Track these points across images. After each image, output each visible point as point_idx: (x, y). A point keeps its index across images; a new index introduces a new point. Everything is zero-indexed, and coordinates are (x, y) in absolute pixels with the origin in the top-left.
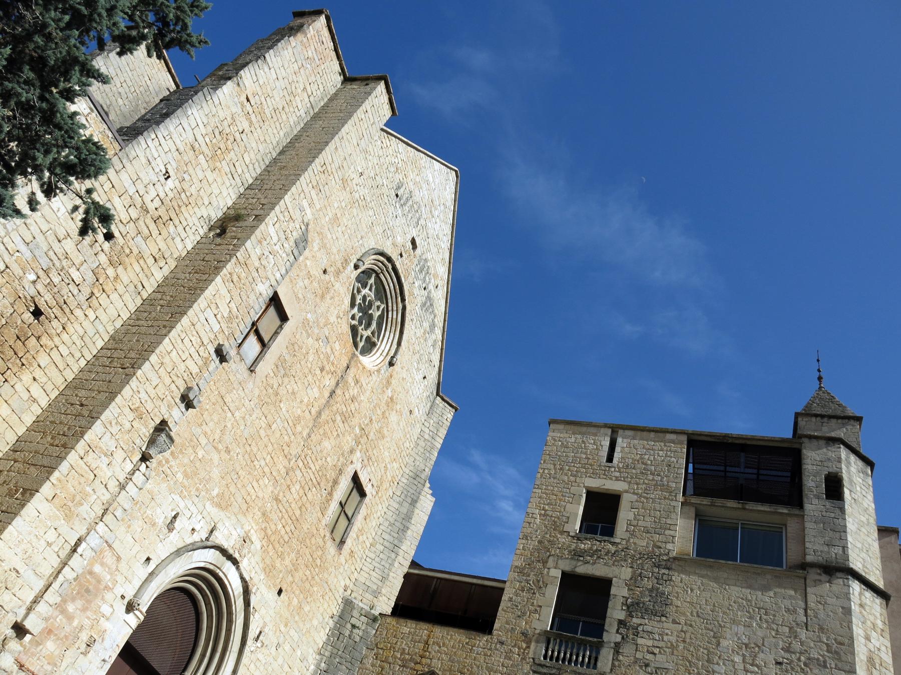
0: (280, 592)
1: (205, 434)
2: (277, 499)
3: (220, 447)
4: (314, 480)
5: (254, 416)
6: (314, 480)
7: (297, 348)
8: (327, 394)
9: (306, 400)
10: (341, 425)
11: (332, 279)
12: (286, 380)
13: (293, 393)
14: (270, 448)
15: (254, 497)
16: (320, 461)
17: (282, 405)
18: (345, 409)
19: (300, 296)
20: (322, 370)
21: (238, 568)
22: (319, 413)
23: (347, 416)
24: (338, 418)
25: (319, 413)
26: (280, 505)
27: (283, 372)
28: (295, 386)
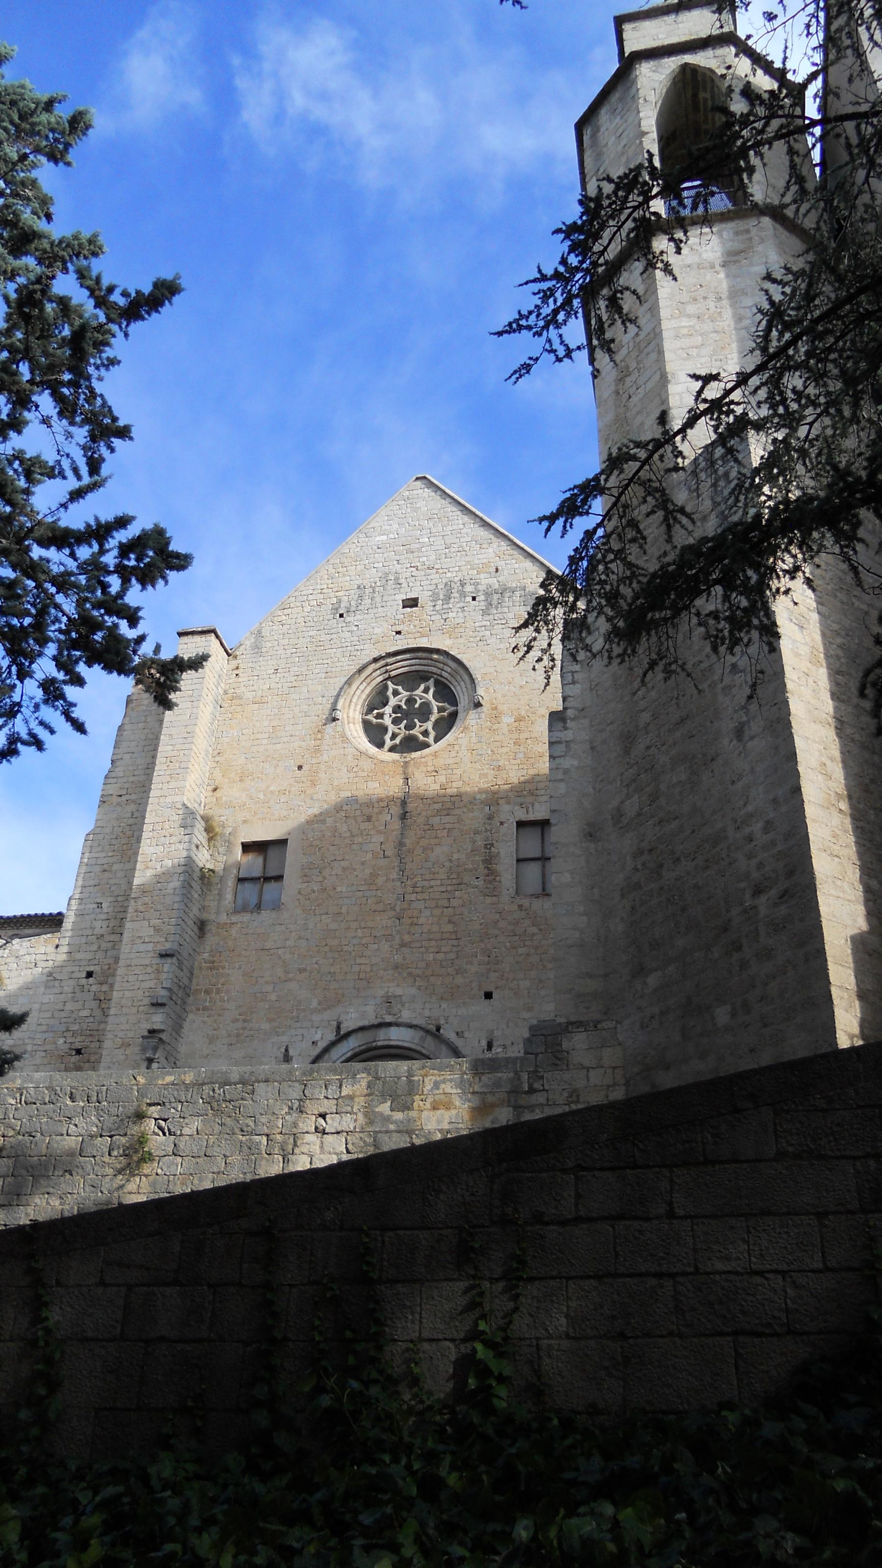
0: (488, 996)
1: (267, 983)
2: (403, 945)
3: (291, 975)
4: (449, 888)
5: (311, 926)
6: (449, 888)
7: (318, 842)
8: (396, 825)
9: (370, 856)
10: (446, 819)
11: (314, 761)
12: (326, 872)
13: (344, 869)
14: (354, 925)
15: (368, 969)
16: (441, 871)
17: (339, 889)
18: (437, 806)
19: (285, 813)
20: (369, 819)
21: (397, 1025)
22: (401, 844)
23: (449, 805)
24: (436, 820)
25: (401, 844)
26: (413, 945)
27: (316, 872)
28: (343, 863)
